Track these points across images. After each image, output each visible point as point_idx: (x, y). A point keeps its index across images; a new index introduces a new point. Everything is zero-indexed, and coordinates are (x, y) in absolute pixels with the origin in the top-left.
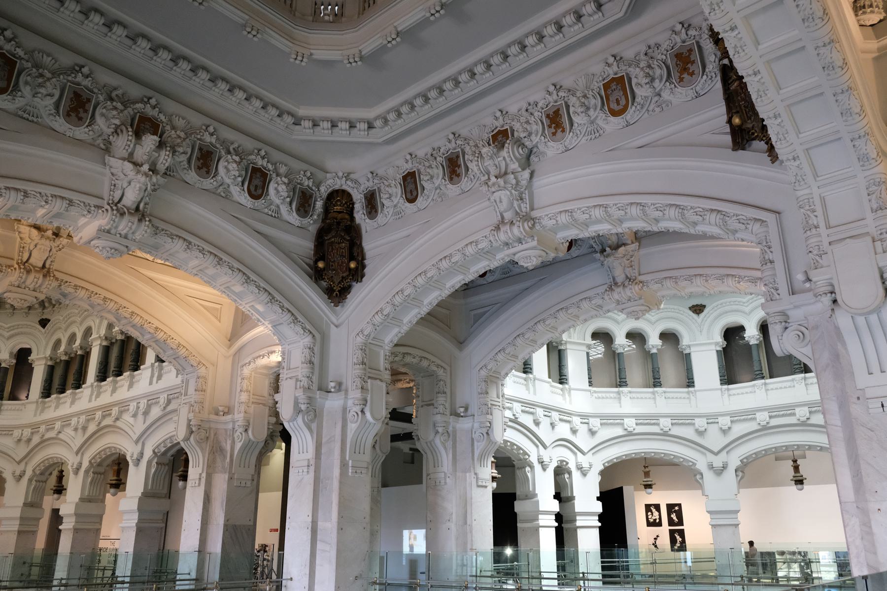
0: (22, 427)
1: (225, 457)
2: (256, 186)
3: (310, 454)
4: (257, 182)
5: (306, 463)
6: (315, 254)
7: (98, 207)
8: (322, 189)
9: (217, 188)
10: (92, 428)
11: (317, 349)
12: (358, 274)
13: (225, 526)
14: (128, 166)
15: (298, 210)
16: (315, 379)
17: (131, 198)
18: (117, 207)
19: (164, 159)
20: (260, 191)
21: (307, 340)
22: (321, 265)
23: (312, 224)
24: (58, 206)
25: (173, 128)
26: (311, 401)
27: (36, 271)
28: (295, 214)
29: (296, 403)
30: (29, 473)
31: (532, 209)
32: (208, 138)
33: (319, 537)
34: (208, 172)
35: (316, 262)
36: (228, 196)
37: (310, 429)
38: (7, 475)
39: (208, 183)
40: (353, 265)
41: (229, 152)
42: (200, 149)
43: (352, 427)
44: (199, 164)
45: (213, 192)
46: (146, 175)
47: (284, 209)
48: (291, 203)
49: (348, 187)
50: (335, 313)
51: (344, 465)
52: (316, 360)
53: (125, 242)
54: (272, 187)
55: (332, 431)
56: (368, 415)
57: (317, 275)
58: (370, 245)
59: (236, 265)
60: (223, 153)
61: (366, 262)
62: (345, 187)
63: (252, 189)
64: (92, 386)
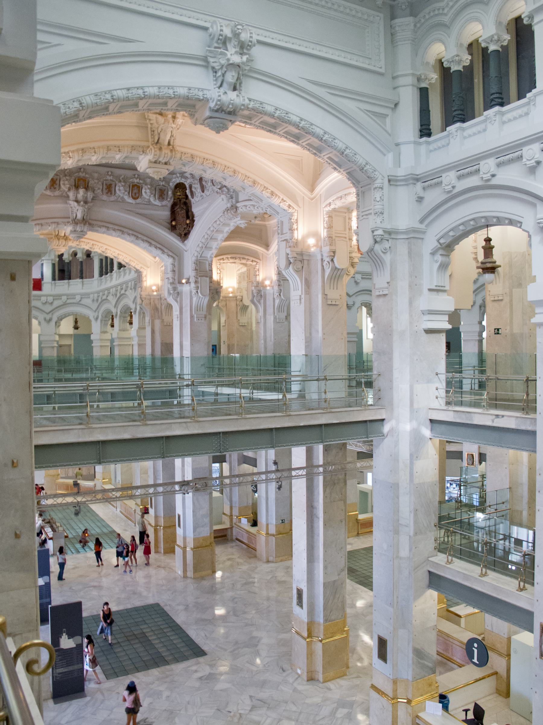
0: (93, 293)
1: (159, 312)
2: (135, 194)
3: (178, 313)
4: (136, 191)
5: (176, 316)
6: (171, 217)
7: (68, 222)
8: (171, 184)
9: (118, 199)
10: (118, 295)
11: (176, 264)
12: (191, 225)
13: (162, 343)
14: (76, 204)
15: (159, 199)
16: (176, 278)
17: (79, 216)
18: (75, 222)
19: (90, 195)
20: (137, 195)
21: (170, 261)
22: (174, 223)
23: (168, 203)
24: (54, 226)
25: (93, 179)
26: (175, 289)
27: (63, 239)
28: (157, 201)
29: (169, 290)
30: (100, 317)
31: (237, 202)
32: (109, 178)
33: (184, 348)
34: (111, 194)
35: (172, 222)
36: (123, 201)
37: (177, 301)
38: (91, 318)
39: (113, 198)
40: (188, 222)
41: (120, 181)
42: (106, 184)
43: (194, 299)
44: (107, 191)
45: (116, 201)
46: (82, 206)
47: (152, 199)
48: (155, 196)
49: (183, 181)
50: (185, 245)
51: (192, 317)
52: (176, 269)
53: (82, 233)
54: (143, 191)
55: (186, 302)
56: (199, 293)
57: (173, 228)
58: (196, 210)
59: (131, 232)
60: (117, 182)
61: (195, 219)
62: (181, 181)
63: (133, 195)
64: (116, 272)
